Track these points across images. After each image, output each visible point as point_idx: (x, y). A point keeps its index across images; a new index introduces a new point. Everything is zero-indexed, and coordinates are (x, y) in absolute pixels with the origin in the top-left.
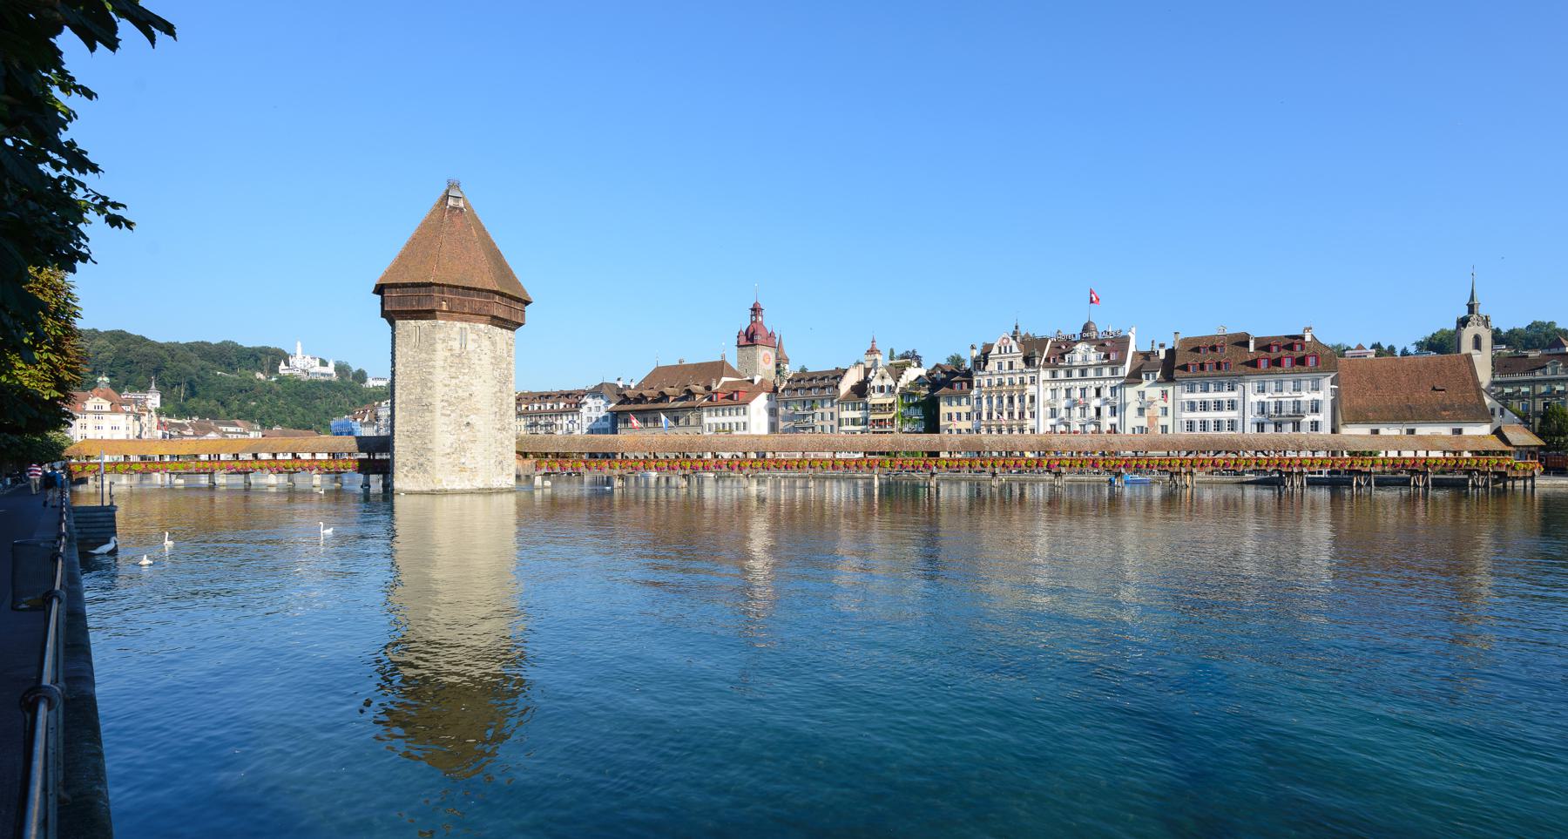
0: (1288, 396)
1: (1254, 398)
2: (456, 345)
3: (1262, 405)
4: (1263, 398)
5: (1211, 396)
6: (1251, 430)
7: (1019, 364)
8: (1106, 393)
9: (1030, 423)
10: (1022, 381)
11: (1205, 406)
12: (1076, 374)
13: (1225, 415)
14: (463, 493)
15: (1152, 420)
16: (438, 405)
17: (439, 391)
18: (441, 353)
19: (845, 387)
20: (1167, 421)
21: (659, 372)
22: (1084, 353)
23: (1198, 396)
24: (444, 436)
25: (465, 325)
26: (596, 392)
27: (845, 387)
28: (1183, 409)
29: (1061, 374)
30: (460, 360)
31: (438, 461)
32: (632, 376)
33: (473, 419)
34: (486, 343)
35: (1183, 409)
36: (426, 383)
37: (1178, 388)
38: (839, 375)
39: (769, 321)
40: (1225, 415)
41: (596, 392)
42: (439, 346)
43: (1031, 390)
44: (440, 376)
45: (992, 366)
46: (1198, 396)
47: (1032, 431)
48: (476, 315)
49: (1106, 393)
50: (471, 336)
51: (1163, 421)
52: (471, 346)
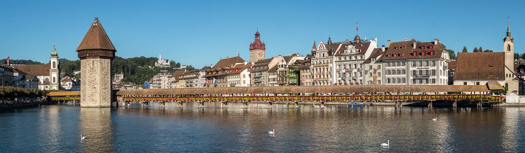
0: (424, 68)
1: (412, 69)
2: (91, 65)
3: (414, 71)
4: (415, 69)
5: (396, 68)
6: (411, 83)
7: (326, 55)
8: (359, 66)
9: (330, 79)
10: (328, 63)
11: (394, 72)
12: (348, 58)
13: (402, 76)
14: (93, 107)
15: (375, 78)
16: (87, 82)
17: (87, 78)
18: (88, 68)
19: (271, 66)
20: (380, 78)
21: (222, 61)
22: (351, 49)
23: (391, 68)
24: (88, 92)
25: (94, 59)
26: (203, 70)
27: (271, 66)
28: (386, 74)
29: (343, 59)
30: (93, 69)
31: (87, 98)
32: (212, 63)
33: (96, 86)
34: (99, 64)
35: (386, 74)
36: (85, 77)
37: (384, 64)
38: (270, 60)
39: (262, 39)
40: (402, 76)
41: (203, 70)
42: (88, 66)
43: (330, 65)
44: (88, 74)
45: (317, 56)
46: (391, 68)
47: (331, 82)
48: (95, 56)
49: (359, 66)
50: (95, 62)
51: (378, 79)
52: (95, 65)
